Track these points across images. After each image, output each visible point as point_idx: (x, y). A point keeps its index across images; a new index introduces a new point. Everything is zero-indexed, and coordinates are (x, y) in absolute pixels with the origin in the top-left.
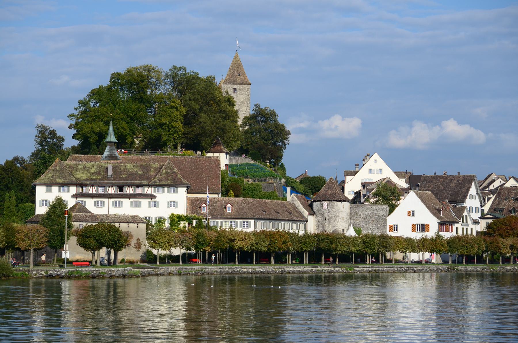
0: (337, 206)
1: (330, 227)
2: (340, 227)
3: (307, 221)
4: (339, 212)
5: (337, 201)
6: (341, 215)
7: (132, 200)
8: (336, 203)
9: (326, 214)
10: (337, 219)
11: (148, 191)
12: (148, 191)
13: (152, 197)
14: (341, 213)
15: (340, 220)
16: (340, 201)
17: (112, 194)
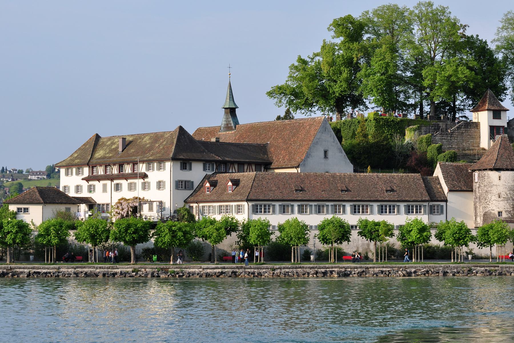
0: (489, 177)
1: (481, 208)
2: (494, 208)
3: (446, 201)
4: (492, 187)
5: (486, 169)
6: (495, 191)
7: (130, 181)
8: (486, 172)
9: (477, 190)
10: (489, 196)
11: (142, 168)
12: (142, 168)
13: (144, 176)
14: (495, 187)
15: (493, 198)
16: (491, 170)
17: (101, 176)
